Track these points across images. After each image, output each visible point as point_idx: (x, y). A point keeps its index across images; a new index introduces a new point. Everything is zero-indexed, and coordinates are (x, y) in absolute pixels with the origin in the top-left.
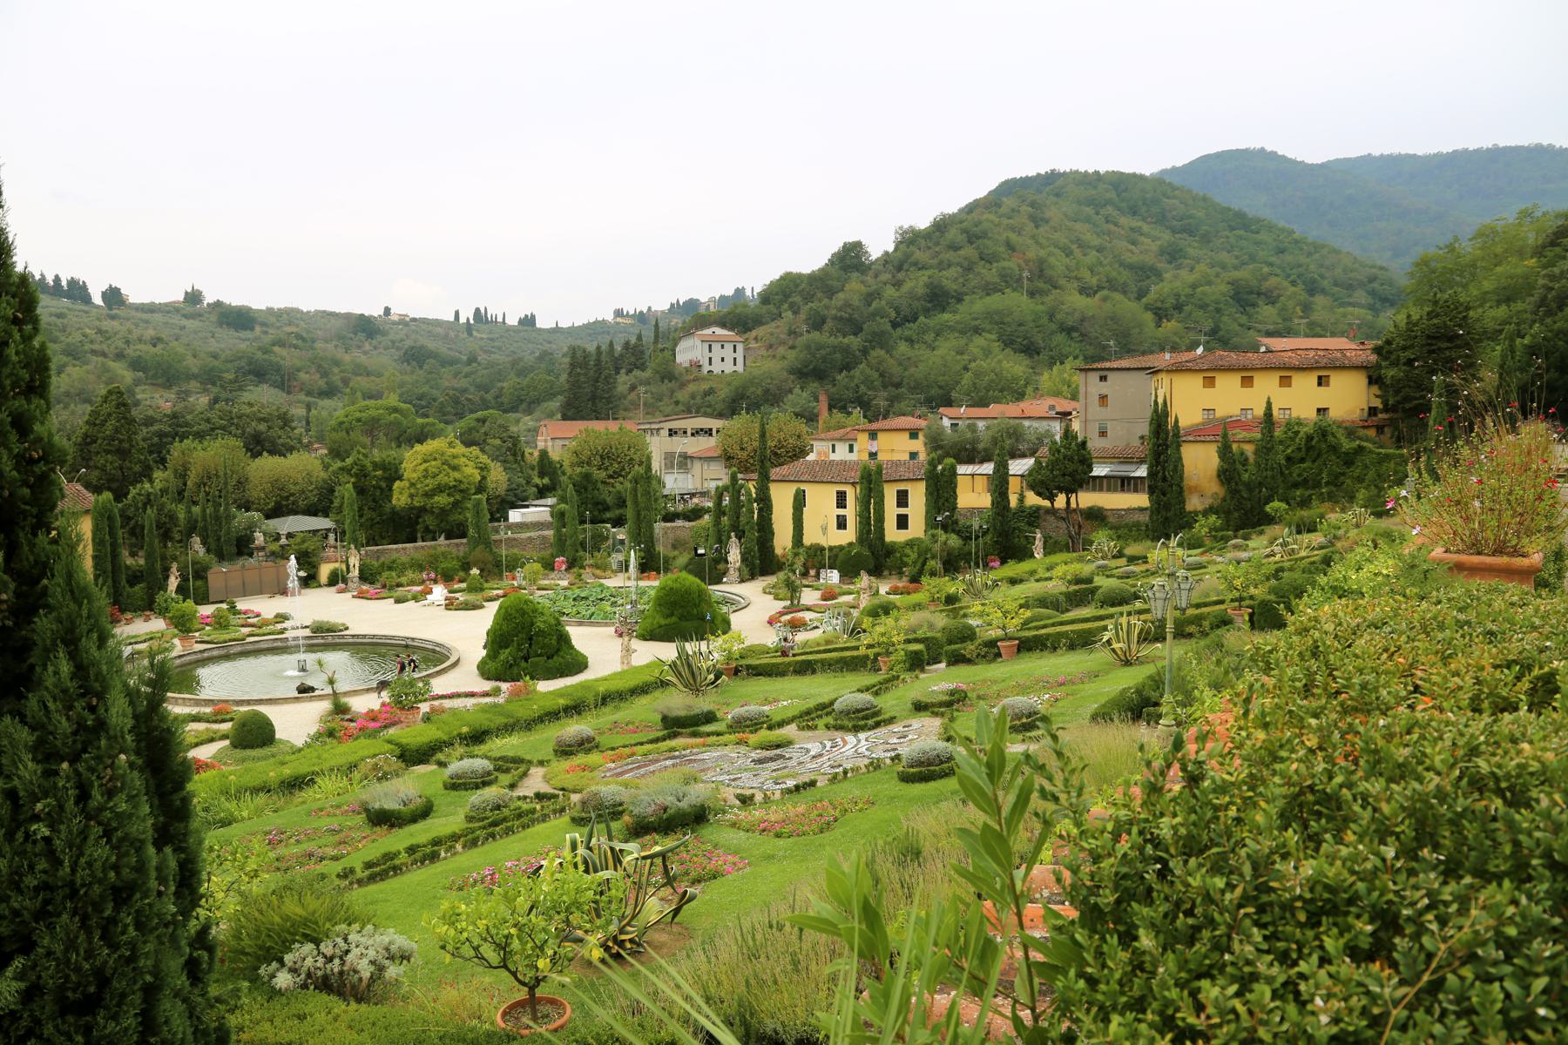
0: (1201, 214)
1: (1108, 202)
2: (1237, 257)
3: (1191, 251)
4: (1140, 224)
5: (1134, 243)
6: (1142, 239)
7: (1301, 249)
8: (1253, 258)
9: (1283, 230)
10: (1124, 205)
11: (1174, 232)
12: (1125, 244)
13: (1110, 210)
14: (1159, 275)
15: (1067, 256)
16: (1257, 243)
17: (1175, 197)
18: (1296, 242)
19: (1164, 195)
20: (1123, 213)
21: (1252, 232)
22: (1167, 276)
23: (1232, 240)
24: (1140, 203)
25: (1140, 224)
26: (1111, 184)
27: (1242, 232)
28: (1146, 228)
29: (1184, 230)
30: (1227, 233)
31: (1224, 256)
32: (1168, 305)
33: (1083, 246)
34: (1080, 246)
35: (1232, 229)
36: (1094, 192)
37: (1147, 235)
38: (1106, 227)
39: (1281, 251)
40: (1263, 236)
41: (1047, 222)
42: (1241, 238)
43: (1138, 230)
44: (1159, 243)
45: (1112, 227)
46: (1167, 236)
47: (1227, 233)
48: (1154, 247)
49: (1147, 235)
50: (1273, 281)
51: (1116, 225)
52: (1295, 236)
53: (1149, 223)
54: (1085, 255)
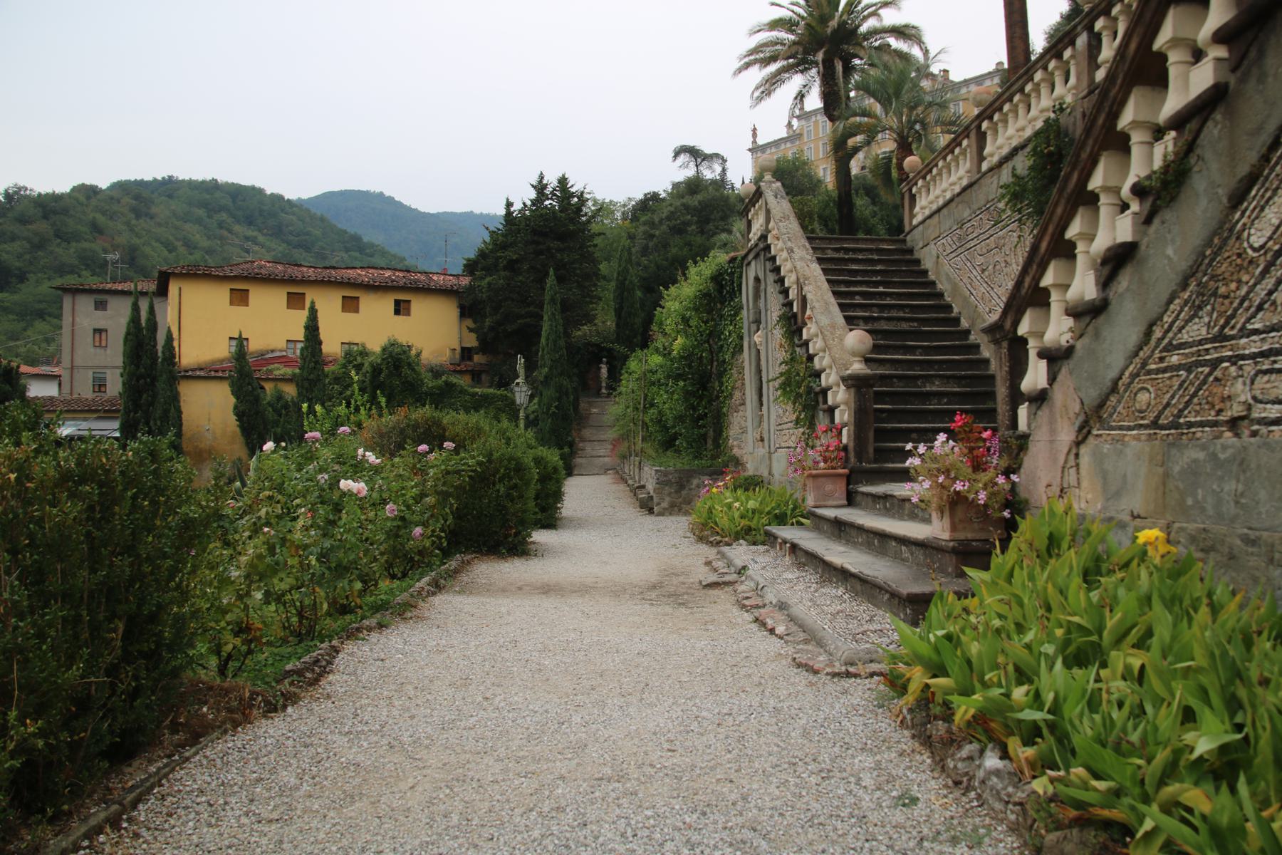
0: (318, 232)
1: (223, 208)
4: (255, 233)
6: (256, 248)
9: (394, 256)
11: (289, 243)
13: (224, 216)
15: (170, 252)
17: (294, 214)
20: (238, 222)
21: (367, 255)
25: (255, 233)
27: (357, 254)
28: (261, 238)
29: (299, 246)
36: (208, 197)
41: (152, 218)
43: (254, 240)
44: (273, 253)
45: (225, 233)
51: (230, 231)
54: (191, 254)
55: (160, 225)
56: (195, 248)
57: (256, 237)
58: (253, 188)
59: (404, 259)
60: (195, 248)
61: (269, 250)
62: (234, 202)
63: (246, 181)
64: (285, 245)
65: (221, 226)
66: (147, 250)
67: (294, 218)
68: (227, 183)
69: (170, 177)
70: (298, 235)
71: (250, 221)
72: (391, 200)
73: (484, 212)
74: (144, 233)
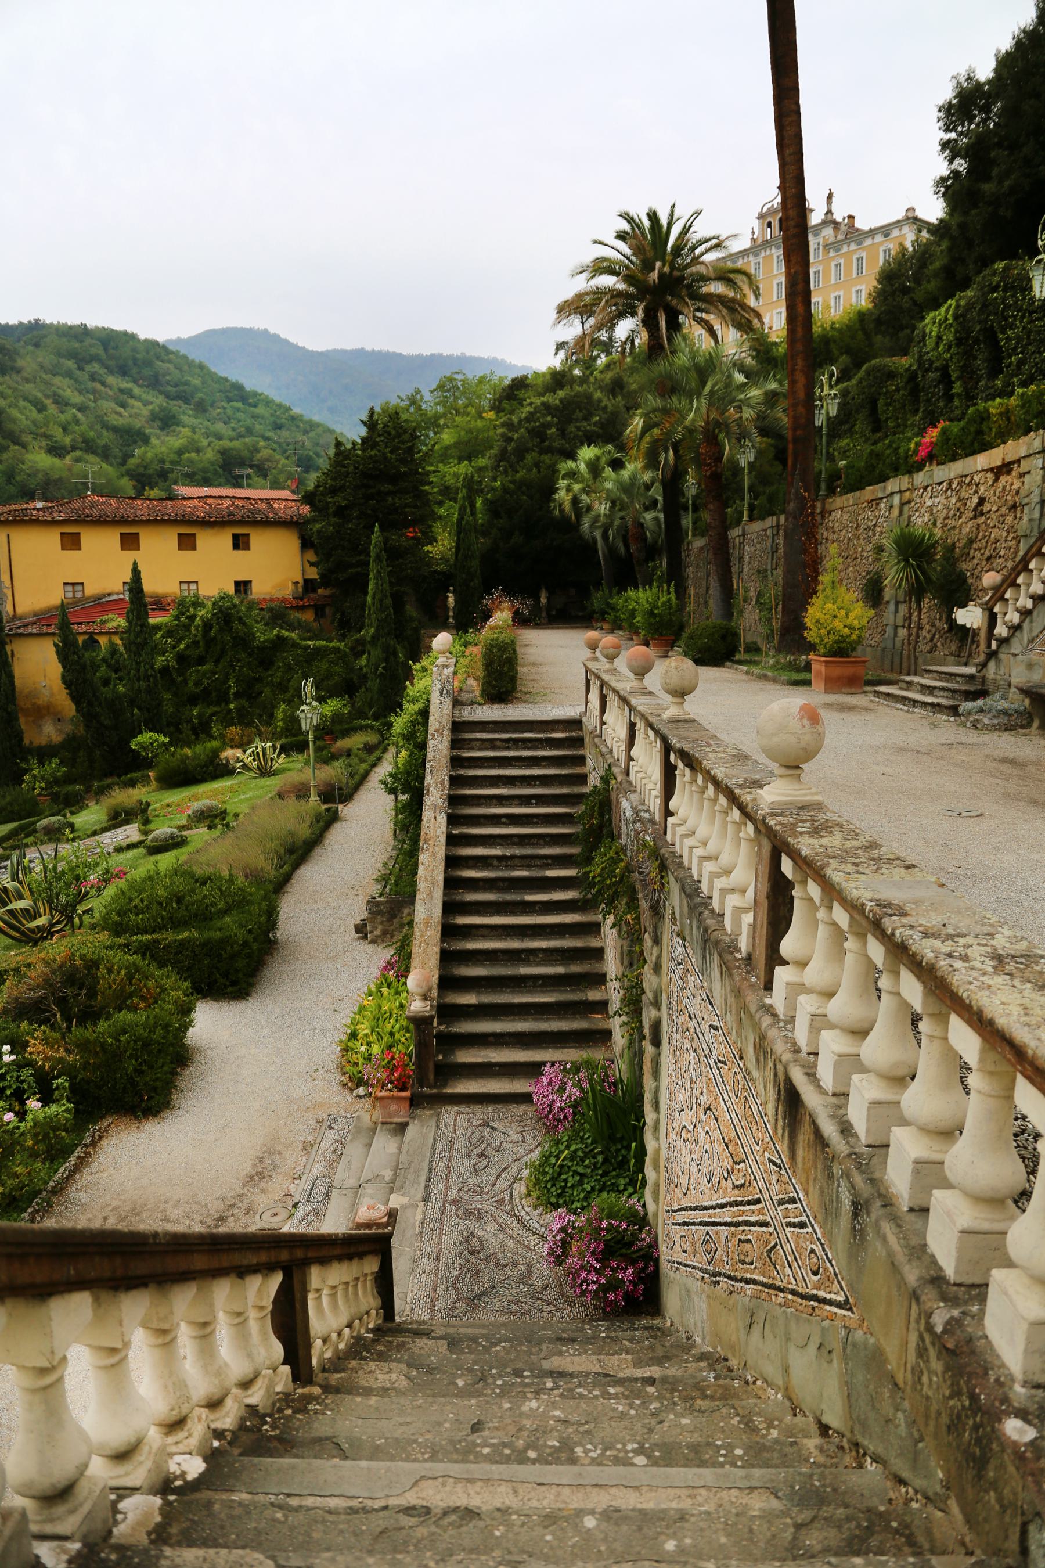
0: (197, 382)
1: (95, 358)
2: (234, 429)
3: (185, 419)
4: (130, 385)
5: (123, 405)
6: (131, 401)
7: (298, 427)
8: (249, 431)
9: (280, 406)
10: (111, 363)
11: (168, 396)
12: (113, 405)
13: (96, 367)
14: (146, 440)
15: (40, 411)
16: (254, 417)
18: (293, 418)
19: (158, 358)
20: (111, 372)
21: (250, 405)
22: (154, 441)
23: (229, 412)
24: (131, 363)
26: (99, 339)
27: (239, 405)
28: (136, 391)
29: (177, 397)
30: (224, 404)
31: (220, 427)
32: (150, 472)
33: (61, 403)
34: (56, 402)
35: (230, 400)
36: (77, 345)
37: (138, 399)
38: (90, 385)
39: (278, 427)
40: (260, 410)
41: (18, 371)
42: (238, 410)
44: (150, 407)
45: (98, 386)
46: (159, 401)
47: (224, 404)
48: (145, 412)
49: (138, 399)
50: (265, 453)
51: (103, 384)
52: (292, 413)
53: (141, 386)
54: (62, 412)
55: (27, 380)
56: (67, 404)
57: (131, 390)
58: (125, 333)
59: (289, 409)
60: (67, 404)
61: (146, 403)
62: (106, 350)
63: (118, 325)
64: (161, 398)
65: (93, 377)
66: (14, 412)
67: (170, 366)
68: (97, 328)
69: (37, 321)
70: (176, 386)
71: (123, 371)
72: (276, 338)
73: (377, 349)
74: (9, 391)
